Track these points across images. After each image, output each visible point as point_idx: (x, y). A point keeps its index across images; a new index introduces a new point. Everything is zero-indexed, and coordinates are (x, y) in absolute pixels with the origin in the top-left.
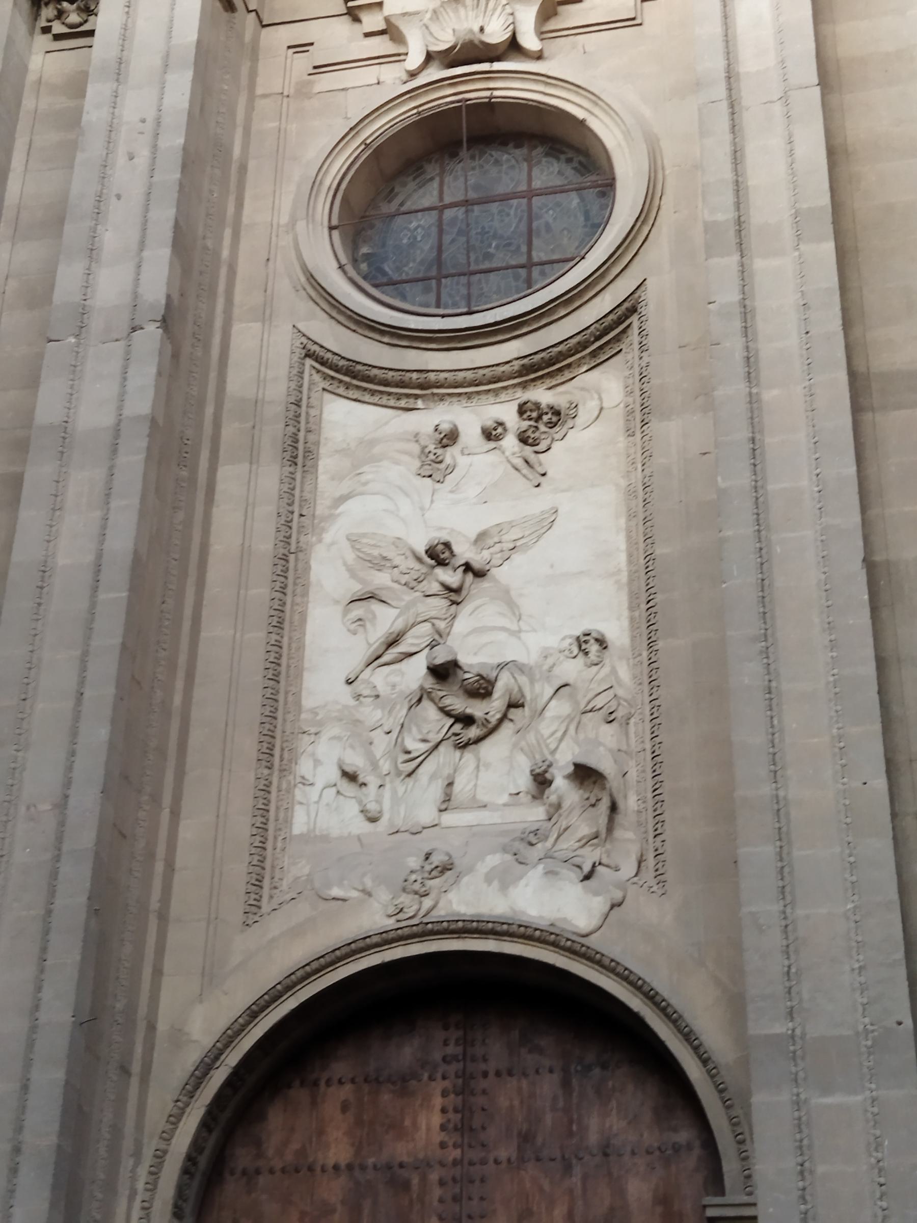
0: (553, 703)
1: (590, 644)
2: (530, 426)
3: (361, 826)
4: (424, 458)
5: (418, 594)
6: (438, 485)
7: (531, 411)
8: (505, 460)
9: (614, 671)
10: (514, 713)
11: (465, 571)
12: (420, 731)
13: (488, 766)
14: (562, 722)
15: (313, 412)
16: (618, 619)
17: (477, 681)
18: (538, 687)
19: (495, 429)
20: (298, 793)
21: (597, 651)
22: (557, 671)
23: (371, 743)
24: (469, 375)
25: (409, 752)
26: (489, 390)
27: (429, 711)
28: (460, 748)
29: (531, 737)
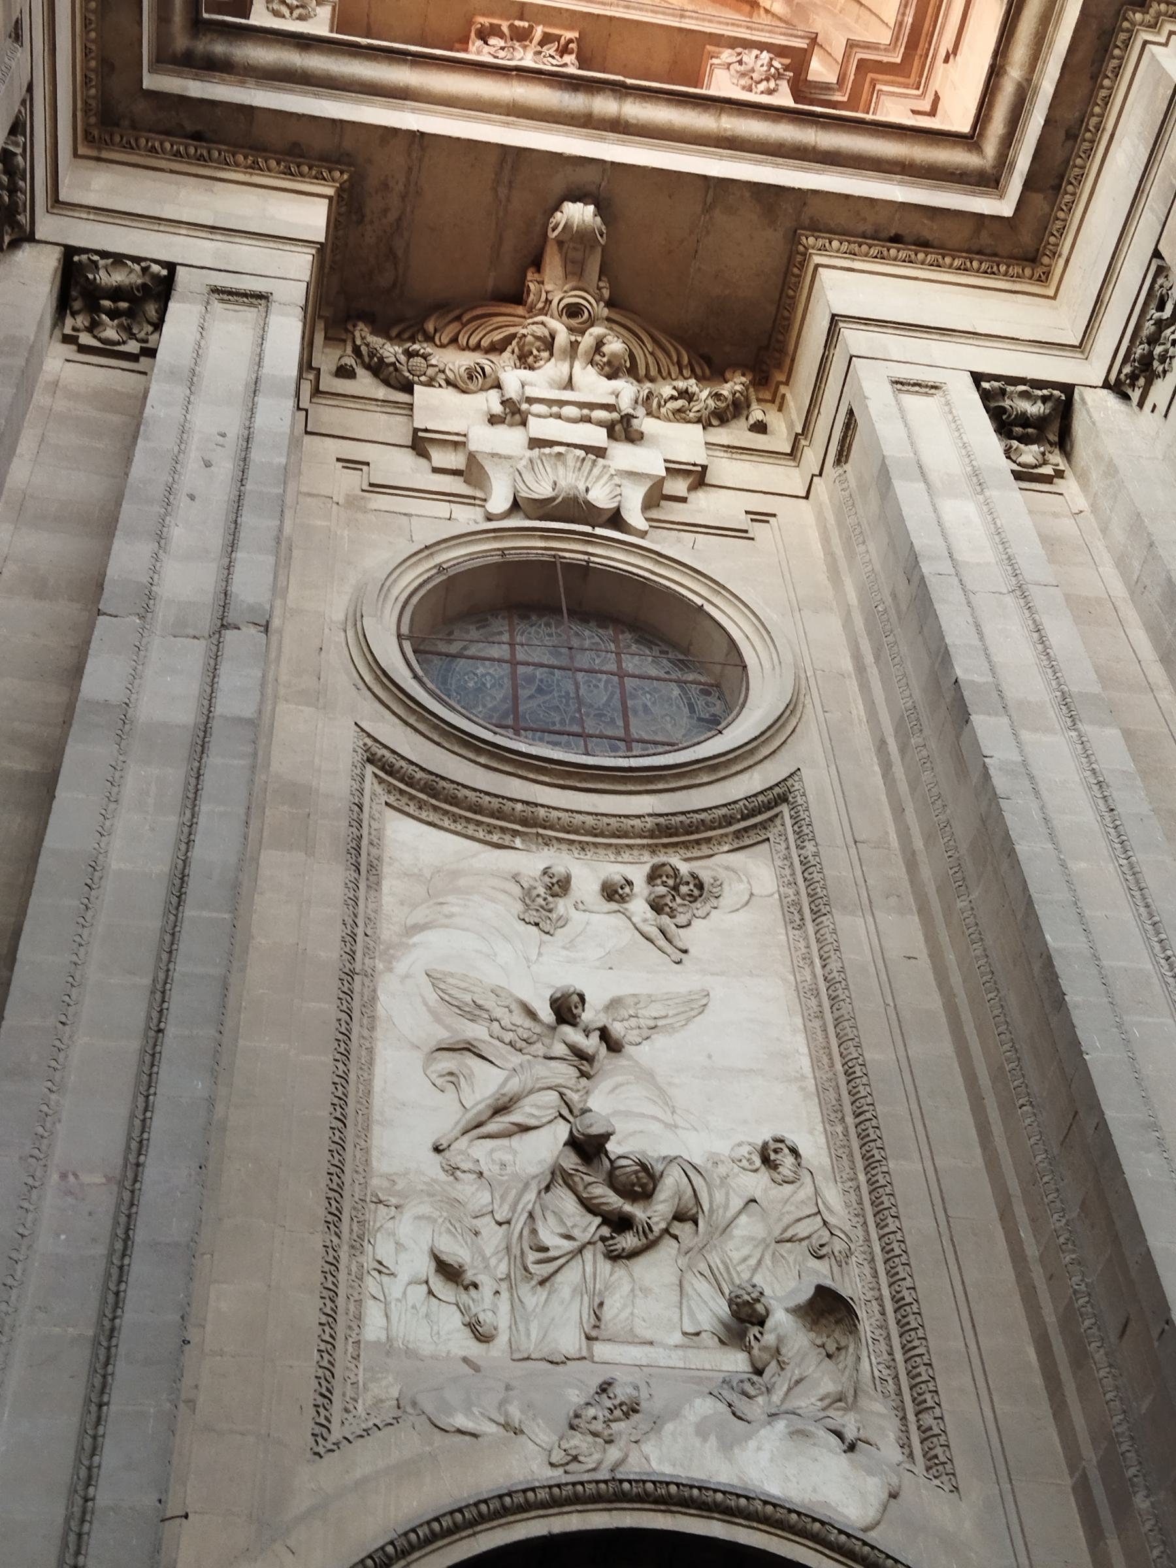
0: (743, 1219)
10: (683, 1229)
12: (562, 1222)
13: (646, 1291)
14: (756, 1247)
15: (375, 825)
17: (636, 1172)
18: (719, 1196)
20: (371, 1284)
23: (476, 1234)
24: (590, 821)
25: (546, 1249)
26: (610, 845)
27: (567, 1202)
29: (715, 1259)
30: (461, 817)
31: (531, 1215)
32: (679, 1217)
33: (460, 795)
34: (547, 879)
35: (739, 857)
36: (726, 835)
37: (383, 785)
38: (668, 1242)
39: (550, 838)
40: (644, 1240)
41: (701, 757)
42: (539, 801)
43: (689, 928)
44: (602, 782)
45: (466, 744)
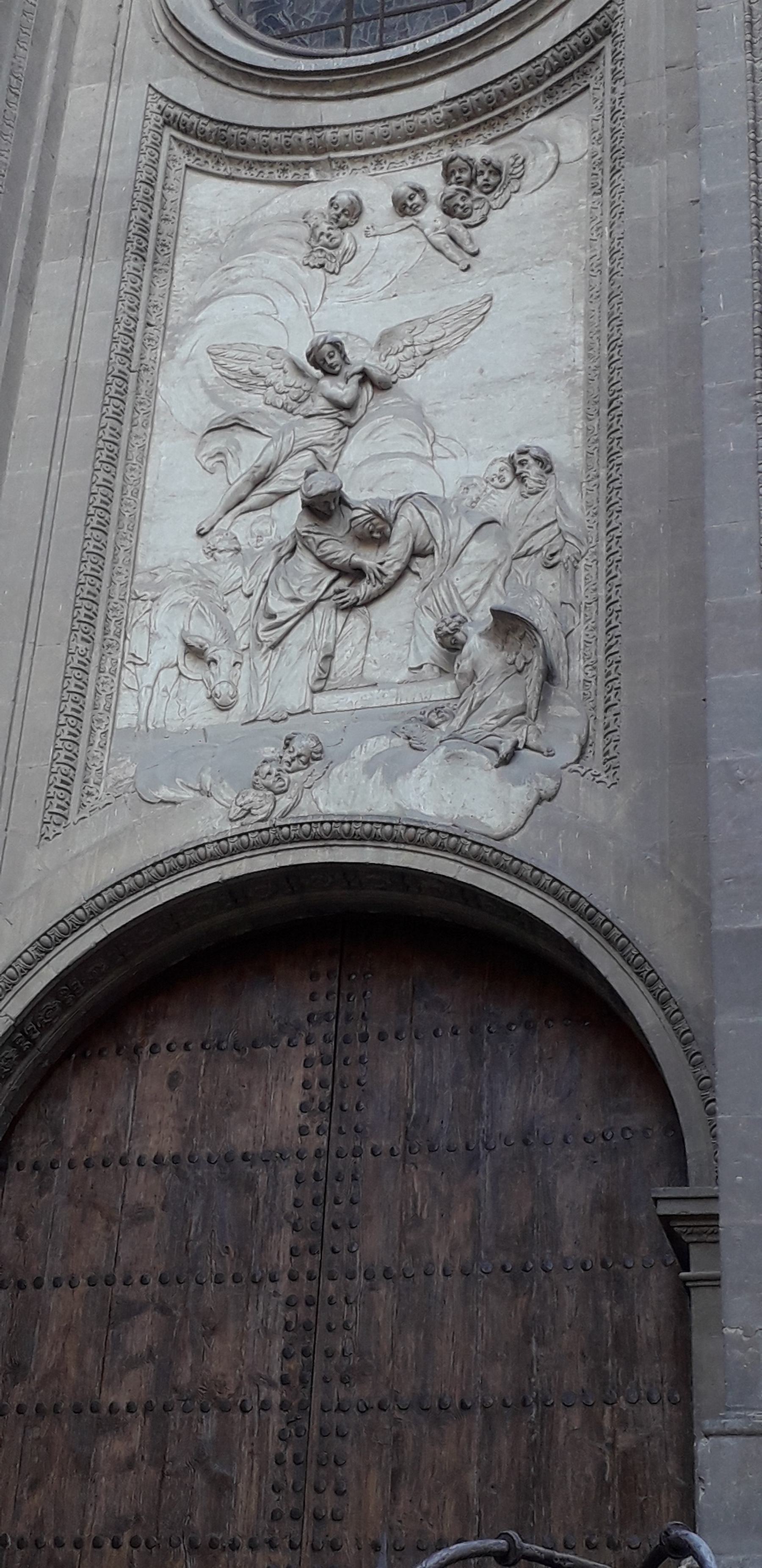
1: (527, 467)
2: (458, 190)
3: (205, 716)
4: (313, 243)
5: (298, 417)
6: (332, 278)
7: (460, 171)
8: (424, 239)
9: (560, 499)
10: (419, 564)
11: (361, 383)
13: (381, 634)
16: (570, 433)
17: (370, 520)
18: (452, 526)
19: (411, 199)
21: (538, 474)
22: (482, 507)
25: (274, 616)
28: (343, 609)
30: (254, 162)
31: (267, 582)
32: (417, 553)
33: (248, 138)
34: (333, 212)
35: (551, 120)
36: (535, 98)
37: (183, 147)
38: (410, 579)
39: (343, 160)
40: (379, 585)
41: (496, 14)
42: (325, 123)
43: (485, 225)
44: (389, 79)
45: (250, 77)
